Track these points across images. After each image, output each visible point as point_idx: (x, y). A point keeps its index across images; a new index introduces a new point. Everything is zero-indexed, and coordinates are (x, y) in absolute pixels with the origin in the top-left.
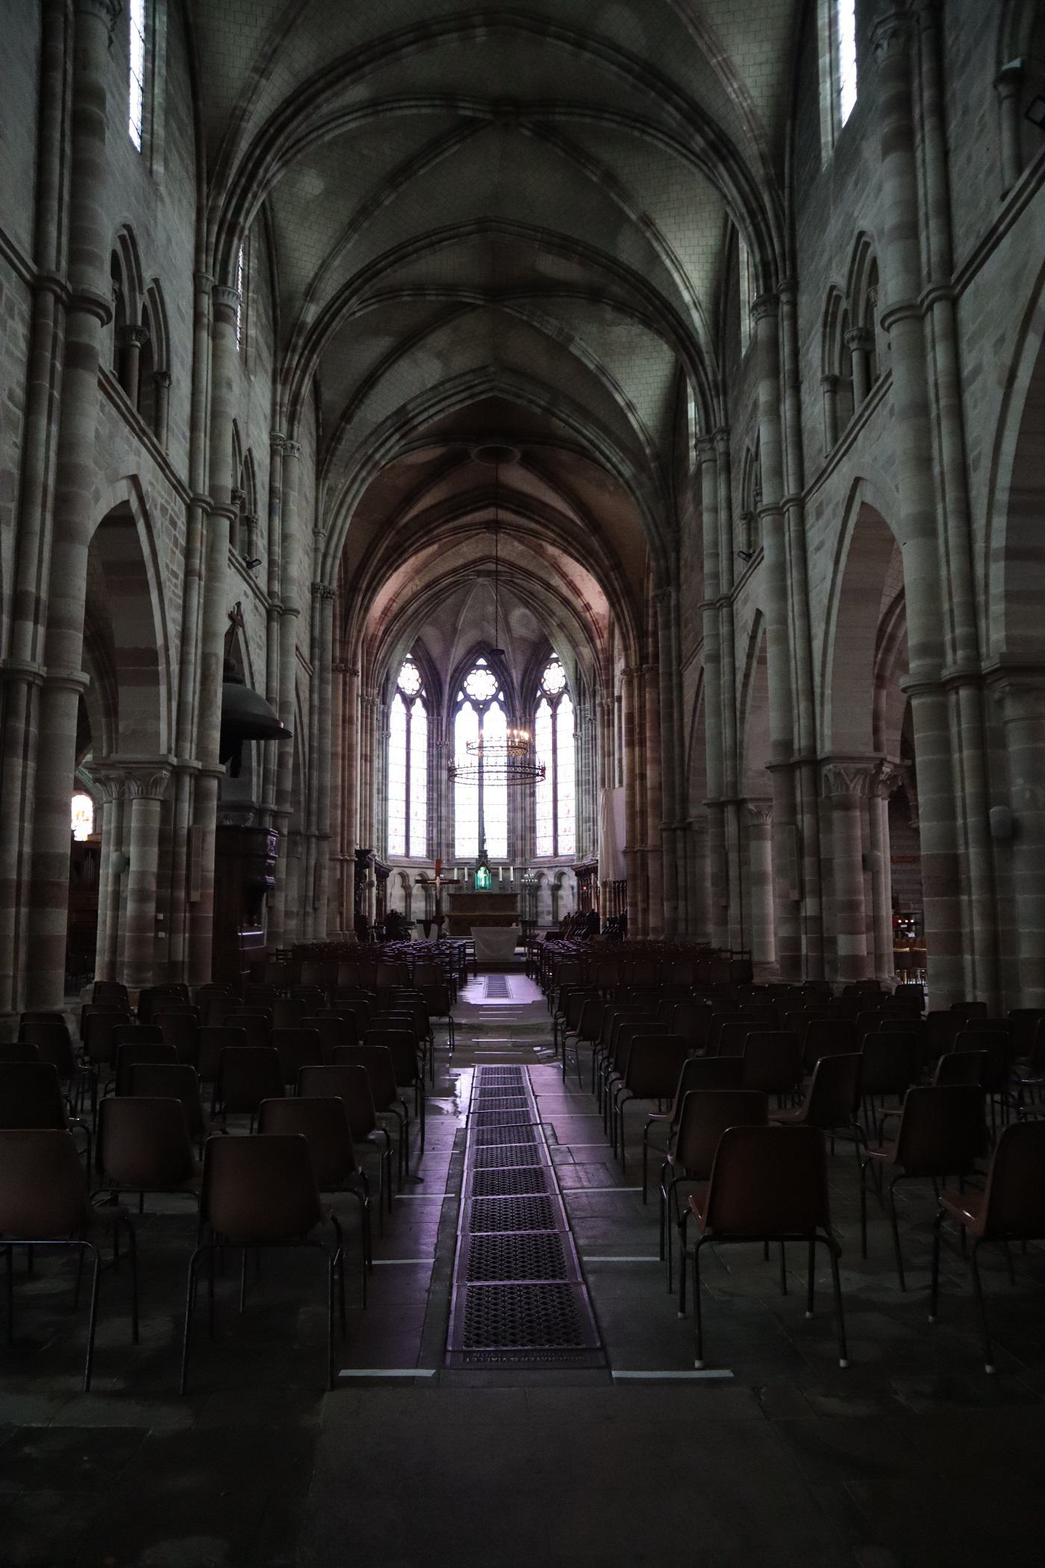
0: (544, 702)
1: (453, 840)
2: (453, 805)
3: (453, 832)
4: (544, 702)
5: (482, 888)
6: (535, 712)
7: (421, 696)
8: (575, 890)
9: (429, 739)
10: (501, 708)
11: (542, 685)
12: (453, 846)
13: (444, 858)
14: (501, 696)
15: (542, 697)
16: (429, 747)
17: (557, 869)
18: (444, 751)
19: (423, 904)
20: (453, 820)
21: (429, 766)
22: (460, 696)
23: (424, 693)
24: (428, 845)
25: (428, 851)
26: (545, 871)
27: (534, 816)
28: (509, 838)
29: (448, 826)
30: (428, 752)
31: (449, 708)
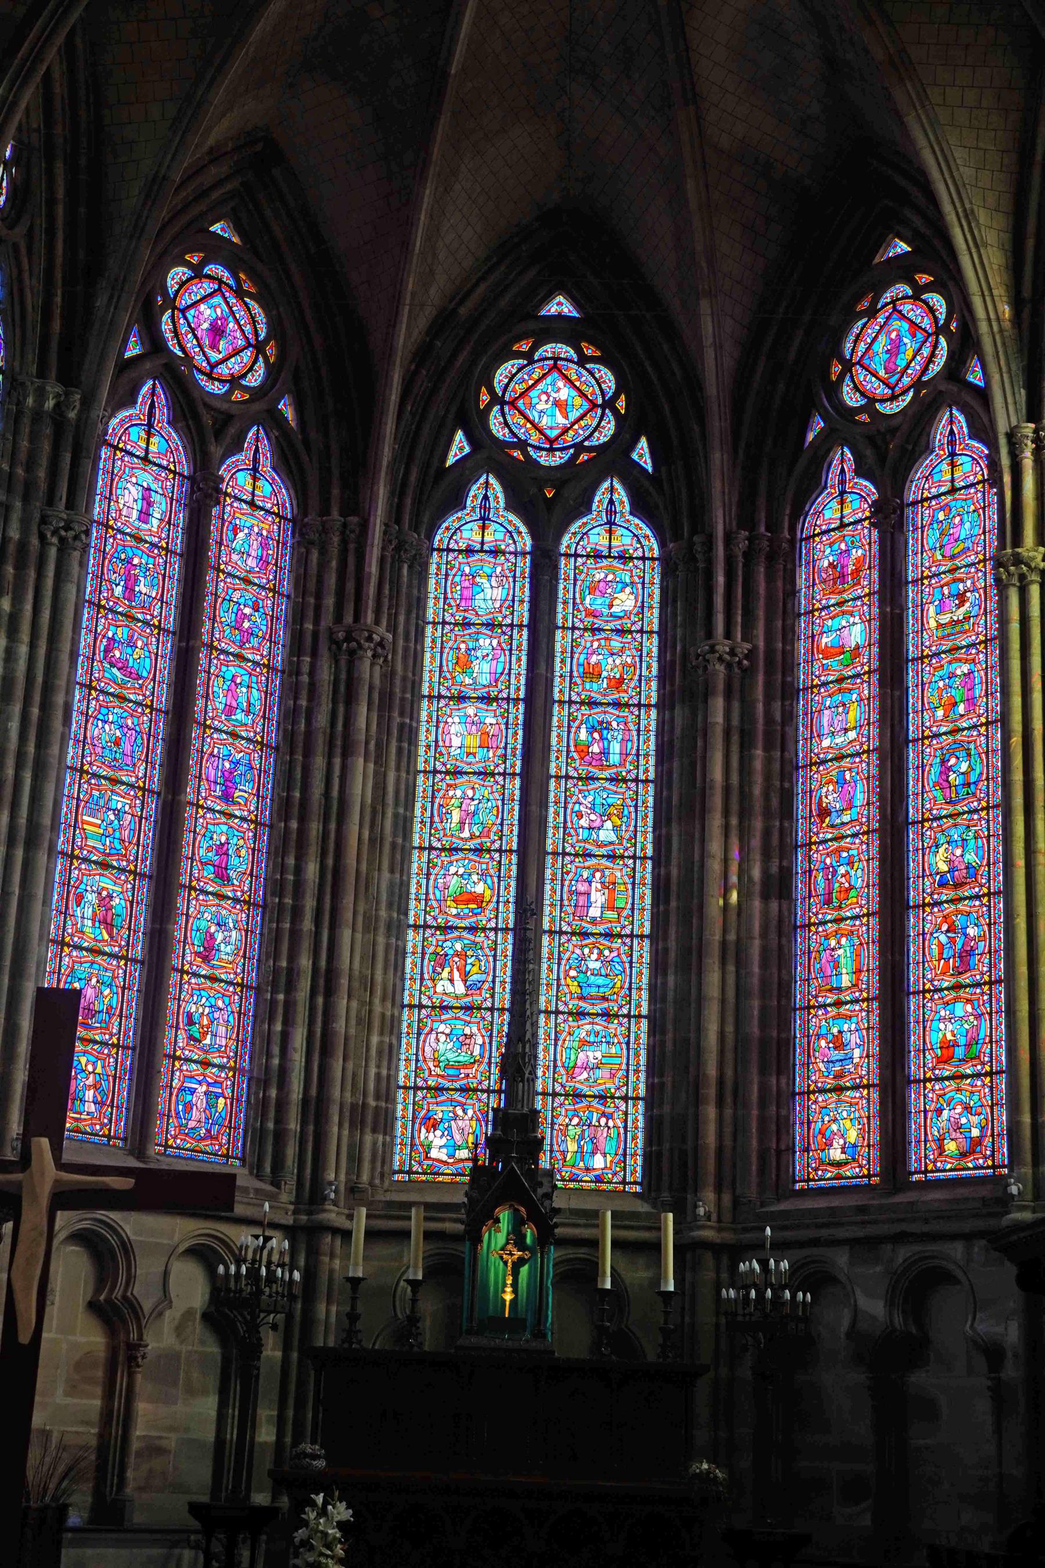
0: (843, 459)
1: (387, 1091)
2: (397, 928)
3: (390, 1054)
4: (843, 459)
5: (498, 1323)
6: (799, 511)
7: (273, 420)
8: (1011, 1371)
9: (298, 616)
10: (641, 507)
11: (834, 389)
12: (384, 1122)
13: (335, 1174)
14: (642, 453)
15: (828, 441)
16: (296, 645)
17: (903, 1253)
18: (368, 671)
19: (209, 1405)
20: (394, 995)
21: (289, 737)
22: (459, 446)
23: (287, 409)
24: (258, 1108)
25: (256, 1136)
26: (841, 1259)
27: (785, 989)
28: (653, 1099)
29: (365, 1023)
30: (292, 671)
31: (398, 492)
